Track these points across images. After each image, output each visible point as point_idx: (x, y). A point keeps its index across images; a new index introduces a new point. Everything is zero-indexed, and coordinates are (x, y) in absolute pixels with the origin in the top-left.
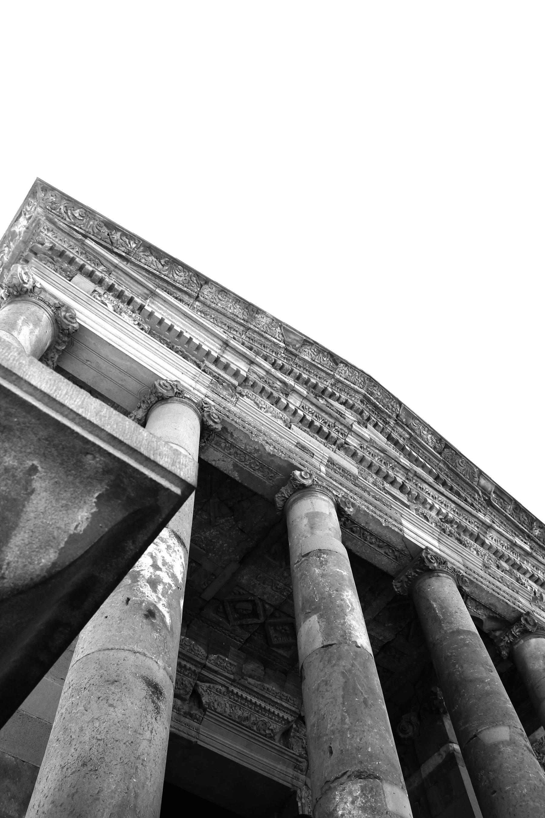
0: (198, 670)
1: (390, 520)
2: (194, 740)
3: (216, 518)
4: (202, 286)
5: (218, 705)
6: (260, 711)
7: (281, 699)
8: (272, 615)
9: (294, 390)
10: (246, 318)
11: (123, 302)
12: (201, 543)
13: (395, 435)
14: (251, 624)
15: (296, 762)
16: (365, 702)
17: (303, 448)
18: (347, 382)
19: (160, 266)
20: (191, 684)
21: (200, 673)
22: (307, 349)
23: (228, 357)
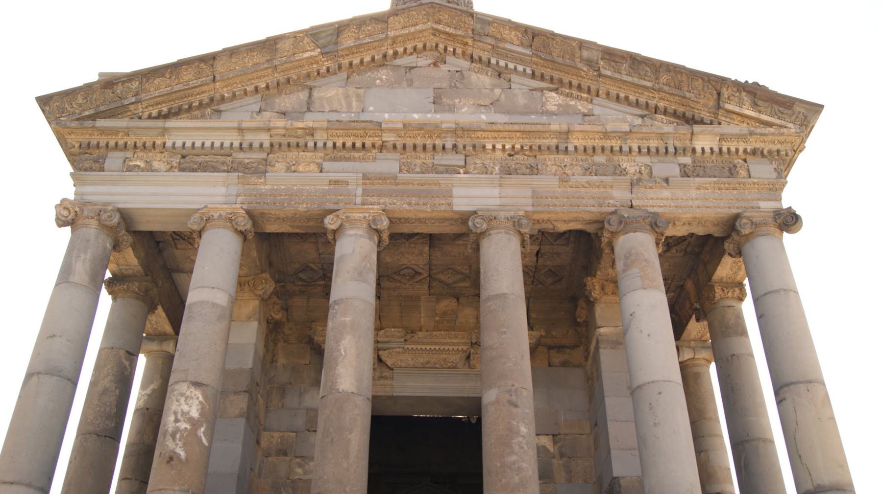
1: (437, 201)
2: (390, 394)
4: (212, 66)
9: (313, 129)
10: (268, 58)
11: (150, 151)
16: (332, 440)
17: (336, 182)
18: (406, 31)
19: (168, 81)
22: (345, 35)
23: (249, 137)
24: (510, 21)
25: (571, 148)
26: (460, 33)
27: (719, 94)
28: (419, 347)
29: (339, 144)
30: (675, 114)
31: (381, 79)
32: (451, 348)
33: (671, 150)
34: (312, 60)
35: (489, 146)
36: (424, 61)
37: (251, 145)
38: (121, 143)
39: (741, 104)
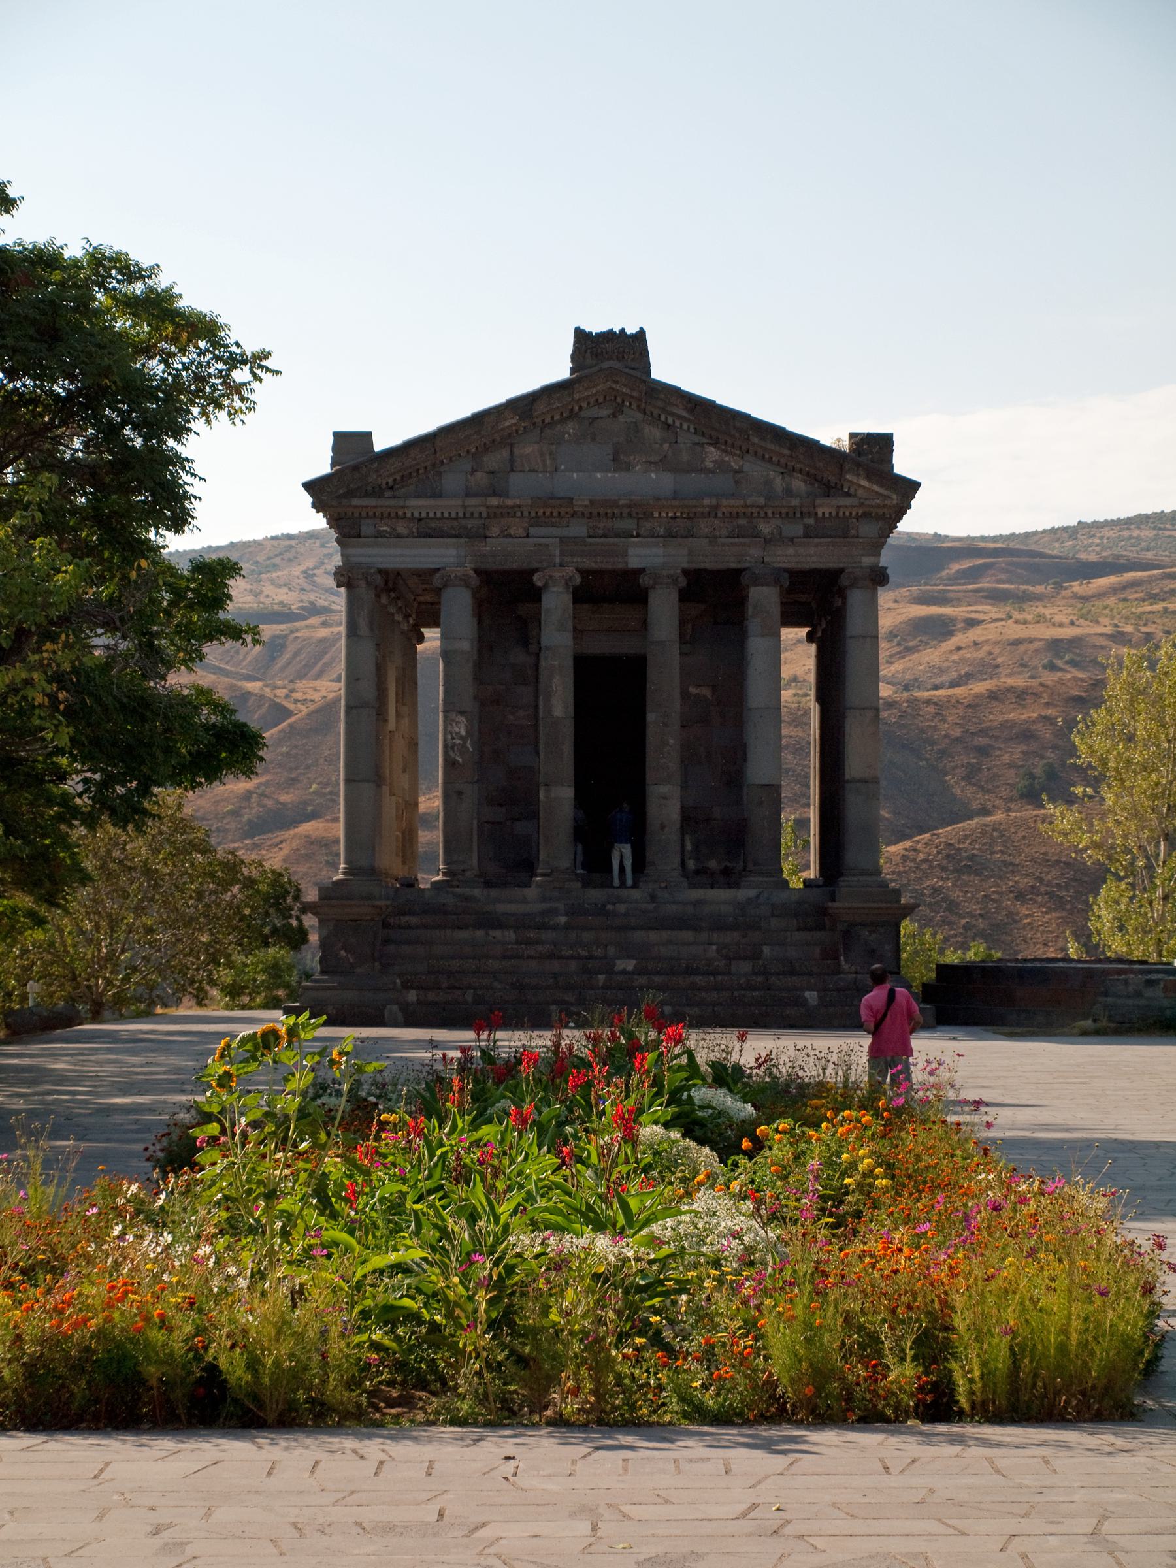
13: (649, 409)
24: (676, 391)
25: (720, 515)
26: (635, 394)
27: (841, 468)
29: (540, 514)
30: (808, 474)
31: (569, 434)
33: (798, 515)
34: (511, 426)
35: (656, 515)
36: (605, 412)
37: (472, 514)
38: (371, 514)
39: (858, 475)
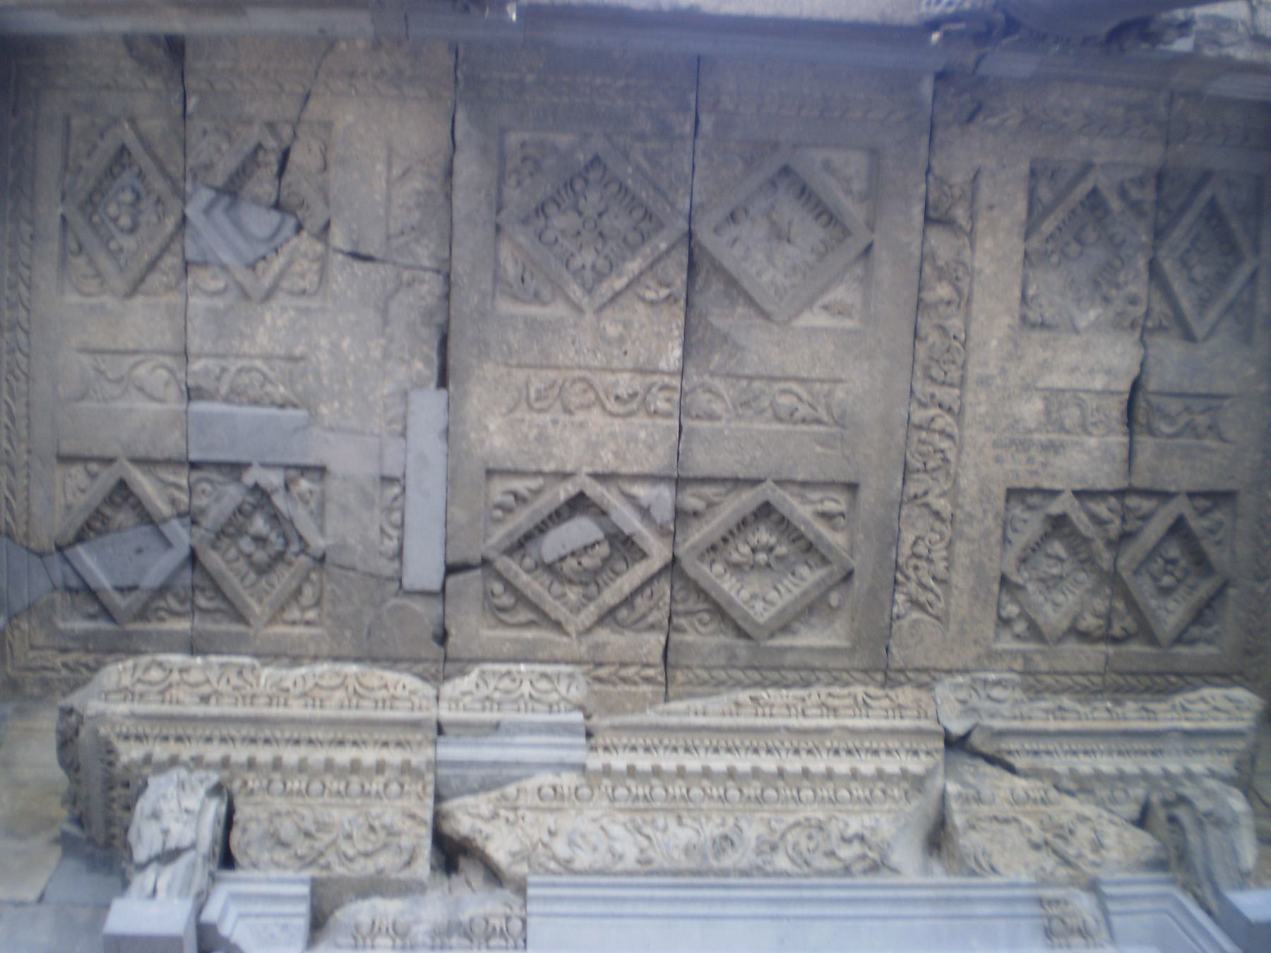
0: (419, 757)
3: (252, 266)
5: (571, 843)
6: (771, 793)
7: (835, 711)
8: (681, 515)
12: (269, 388)
14: (638, 591)
15: (1036, 910)
20: (413, 816)
21: (436, 764)
28: (669, 762)
32: (842, 766)
